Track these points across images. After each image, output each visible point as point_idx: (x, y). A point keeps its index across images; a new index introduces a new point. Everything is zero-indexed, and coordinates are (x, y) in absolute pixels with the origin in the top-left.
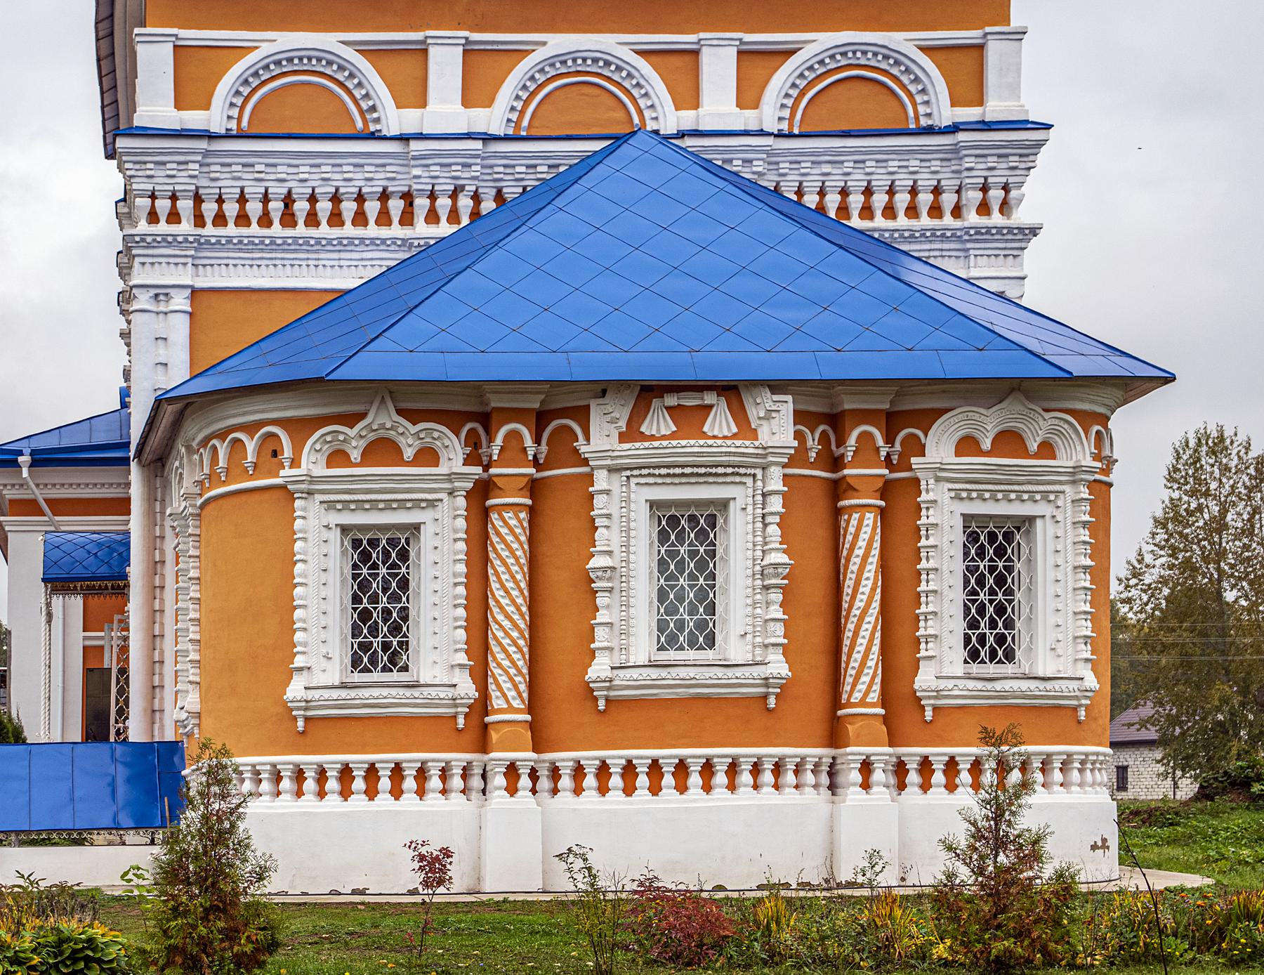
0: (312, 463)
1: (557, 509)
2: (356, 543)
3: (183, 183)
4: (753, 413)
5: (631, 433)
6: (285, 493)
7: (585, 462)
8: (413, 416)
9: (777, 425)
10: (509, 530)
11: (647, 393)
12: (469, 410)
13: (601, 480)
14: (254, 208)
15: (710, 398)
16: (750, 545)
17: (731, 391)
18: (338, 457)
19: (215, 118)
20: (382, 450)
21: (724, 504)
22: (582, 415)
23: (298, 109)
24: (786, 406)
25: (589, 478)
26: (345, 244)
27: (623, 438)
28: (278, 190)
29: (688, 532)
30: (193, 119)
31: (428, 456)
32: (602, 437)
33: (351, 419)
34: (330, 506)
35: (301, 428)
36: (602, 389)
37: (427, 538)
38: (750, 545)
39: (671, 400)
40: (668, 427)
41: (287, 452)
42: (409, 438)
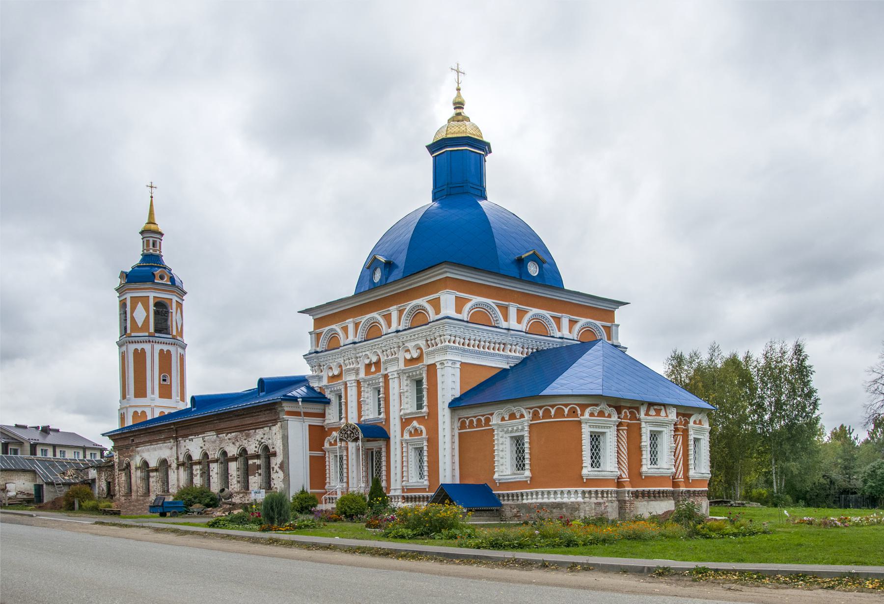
0: (587, 415)
1: (634, 432)
3: (459, 333)
4: (668, 411)
5: (647, 414)
6: (580, 422)
7: (639, 420)
8: (610, 406)
9: (673, 415)
10: (624, 434)
11: (651, 404)
12: (617, 405)
13: (643, 425)
14: (472, 342)
16: (666, 442)
17: (664, 405)
18: (592, 415)
19: (465, 316)
20: (601, 414)
21: (660, 432)
22: (638, 409)
23: (481, 318)
24: (674, 411)
25: (640, 424)
26: (494, 355)
27: (646, 415)
28: (478, 338)
29: (654, 436)
30: (459, 316)
31: (609, 416)
32: (642, 415)
33: (597, 405)
34: (590, 426)
35: (583, 407)
36: (642, 403)
37: (608, 435)
38: (666, 442)
39: (656, 407)
40: (654, 413)
41: (579, 412)
42: (608, 410)
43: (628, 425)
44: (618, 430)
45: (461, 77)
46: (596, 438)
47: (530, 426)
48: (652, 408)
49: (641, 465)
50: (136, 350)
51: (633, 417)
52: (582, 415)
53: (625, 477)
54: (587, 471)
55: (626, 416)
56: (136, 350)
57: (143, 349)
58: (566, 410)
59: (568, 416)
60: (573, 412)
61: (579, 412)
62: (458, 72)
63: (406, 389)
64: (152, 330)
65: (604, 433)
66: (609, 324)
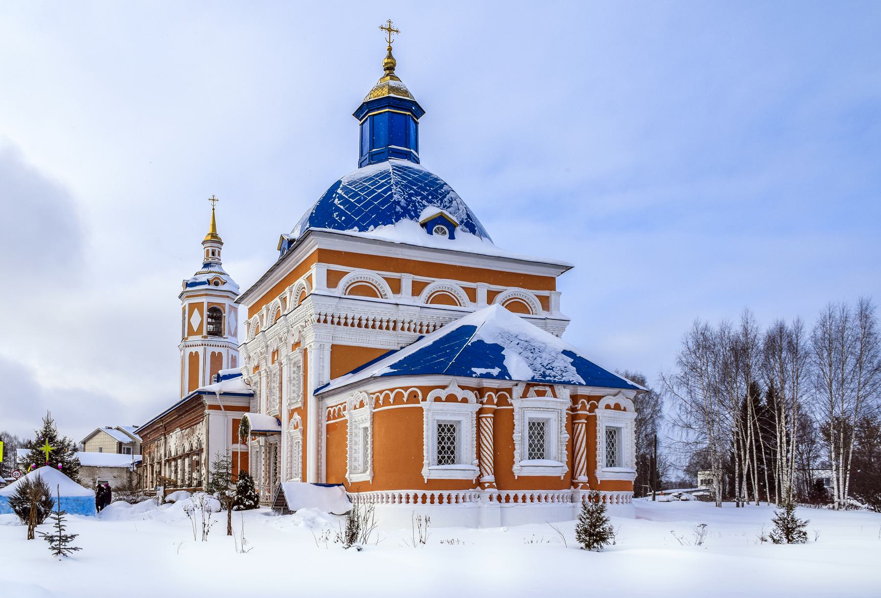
2: (440, 426)
7: (511, 405)
15: (547, 389)
20: (451, 398)
33: (444, 387)
39: (536, 388)
41: (420, 398)
43: (495, 412)
44: (479, 419)
45: (394, 36)
46: (612, 433)
47: (374, 415)
48: (531, 389)
49: (514, 463)
50: (191, 353)
51: (502, 400)
52: (424, 399)
53: (489, 478)
54: (431, 470)
55: (490, 400)
56: (191, 353)
57: (220, 354)
58: (406, 395)
59: (408, 402)
60: (413, 397)
61: (420, 398)
62: (390, 30)
63: (293, 375)
64: (205, 333)
65: (459, 422)
66: (545, 293)
